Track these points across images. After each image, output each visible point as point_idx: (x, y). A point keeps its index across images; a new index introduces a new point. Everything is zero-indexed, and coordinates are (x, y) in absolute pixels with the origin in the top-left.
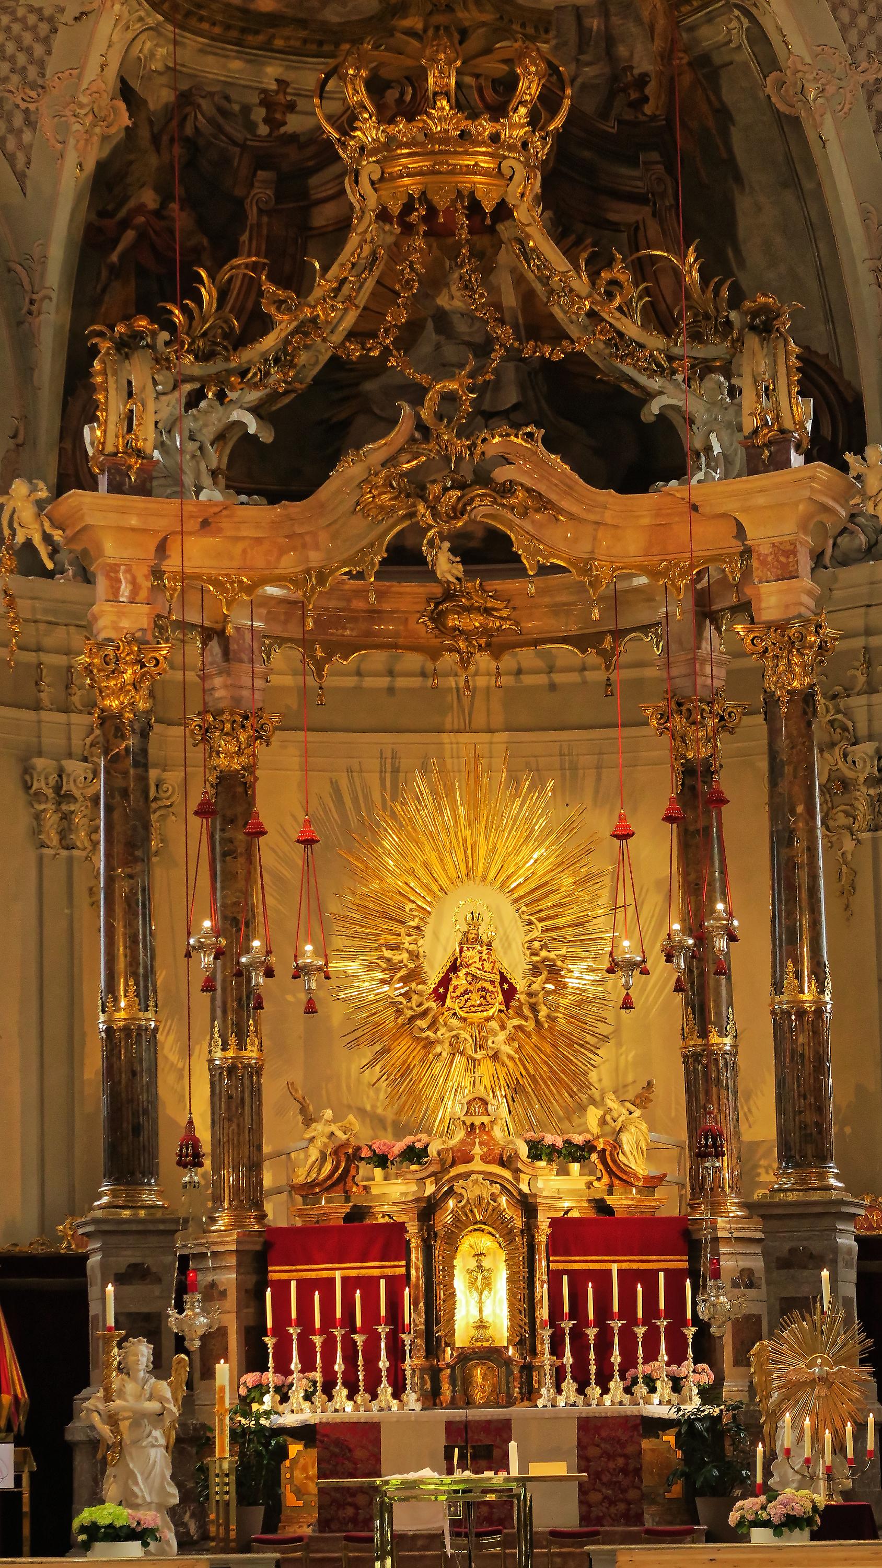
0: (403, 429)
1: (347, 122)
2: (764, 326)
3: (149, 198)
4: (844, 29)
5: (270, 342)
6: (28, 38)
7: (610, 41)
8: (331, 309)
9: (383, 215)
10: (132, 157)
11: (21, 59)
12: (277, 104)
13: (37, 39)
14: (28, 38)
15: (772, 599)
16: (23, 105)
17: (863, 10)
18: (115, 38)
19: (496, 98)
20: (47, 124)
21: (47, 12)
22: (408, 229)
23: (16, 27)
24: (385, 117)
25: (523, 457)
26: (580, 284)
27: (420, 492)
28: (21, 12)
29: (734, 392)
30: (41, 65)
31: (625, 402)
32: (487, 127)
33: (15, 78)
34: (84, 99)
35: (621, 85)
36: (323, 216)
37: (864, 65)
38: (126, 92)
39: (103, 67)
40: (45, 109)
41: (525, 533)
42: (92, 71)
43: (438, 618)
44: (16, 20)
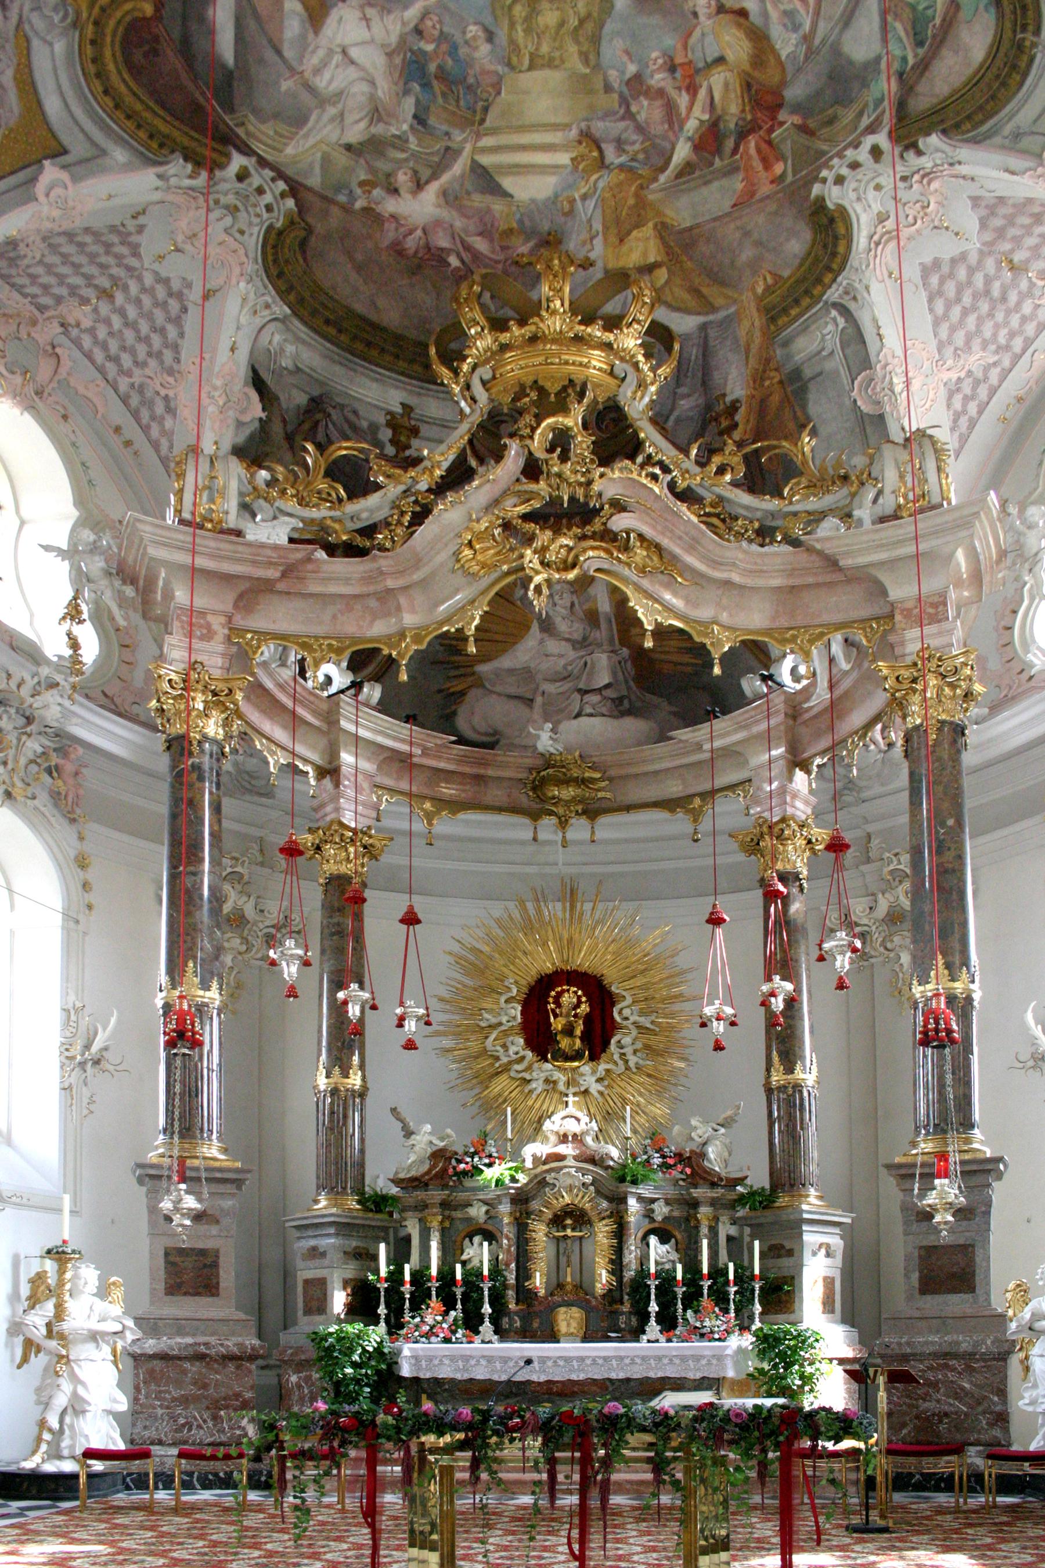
4: (937, 323)
6: (159, 316)
10: (267, 449)
11: (156, 340)
13: (169, 320)
14: (159, 316)
16: (163, 392)
17: (958, 300)
18: (243, 320)
20: (186, 412)
21: (176, 285)
23: (147, 301)
28: (148, 280)
30: (176, 348)
33: (153, 363)
34: (218, 383)
37: (950, 362)
38: (258, 383)
39: (233, 350)
40: (184, 395)
42: (223, 355)
44: (144, 290)
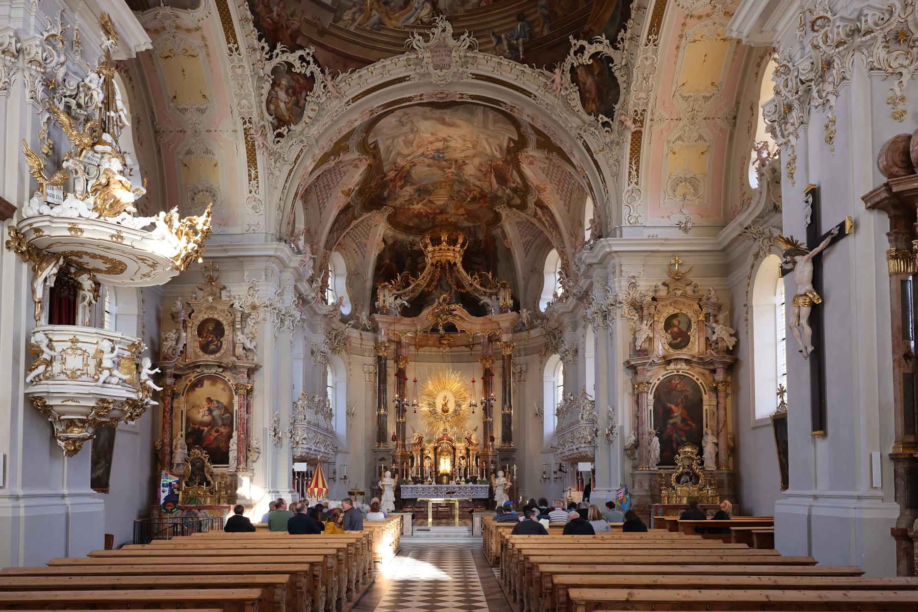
0: (436, 303)
1: (426, 247)
2: (504, 286)
3: (388, 261)
5: (410, 287)
7: (475, 234)
8: (423, 279)
9: (432, 265)
12: (412, 244)
15: (505, 338)
19: (452, 242)
22: (437, 267)
24: (433, 245)
25: (459, 310)
26: (469, 278)
27: (439, 316)
29: (498, 299)
31: (476, 301)
32: (452, 247)
35: (477, 242)
36: (420, 266)
38: (384, 240)
40: (368, 244)
41: (459, 325)
43: (440, 341)
